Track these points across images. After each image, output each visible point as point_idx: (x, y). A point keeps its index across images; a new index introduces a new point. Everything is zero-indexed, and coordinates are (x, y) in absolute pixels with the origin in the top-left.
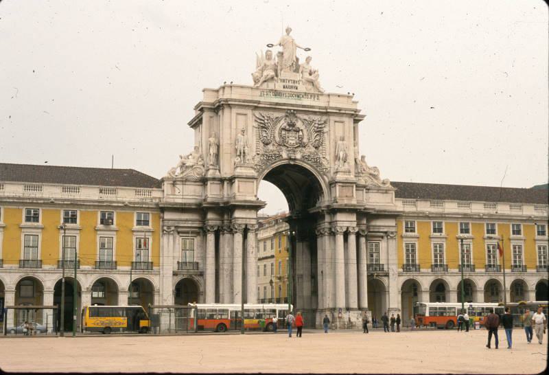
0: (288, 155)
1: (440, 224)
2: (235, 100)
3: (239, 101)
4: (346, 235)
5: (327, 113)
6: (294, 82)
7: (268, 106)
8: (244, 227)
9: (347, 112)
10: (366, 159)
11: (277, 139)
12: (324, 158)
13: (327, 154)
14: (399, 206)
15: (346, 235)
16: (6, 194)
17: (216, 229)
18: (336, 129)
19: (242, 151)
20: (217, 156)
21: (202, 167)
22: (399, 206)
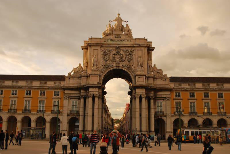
1: (193, 93)
2: (92, 44)
3: (94, 44)
4: (141, 98)
5: (134, 47)
6: (120, 35)
7: (107, 45)
8: (92, 95)
10: (156, 66)
11: (111, 58)
13: (134, 63)
14: (172, 85)
15: (141, 98)
16: (5, 85)
17: (84, 97)
18: (140, 53)
19: (94, 64)
20: (87, 67)
22: (172, 85)
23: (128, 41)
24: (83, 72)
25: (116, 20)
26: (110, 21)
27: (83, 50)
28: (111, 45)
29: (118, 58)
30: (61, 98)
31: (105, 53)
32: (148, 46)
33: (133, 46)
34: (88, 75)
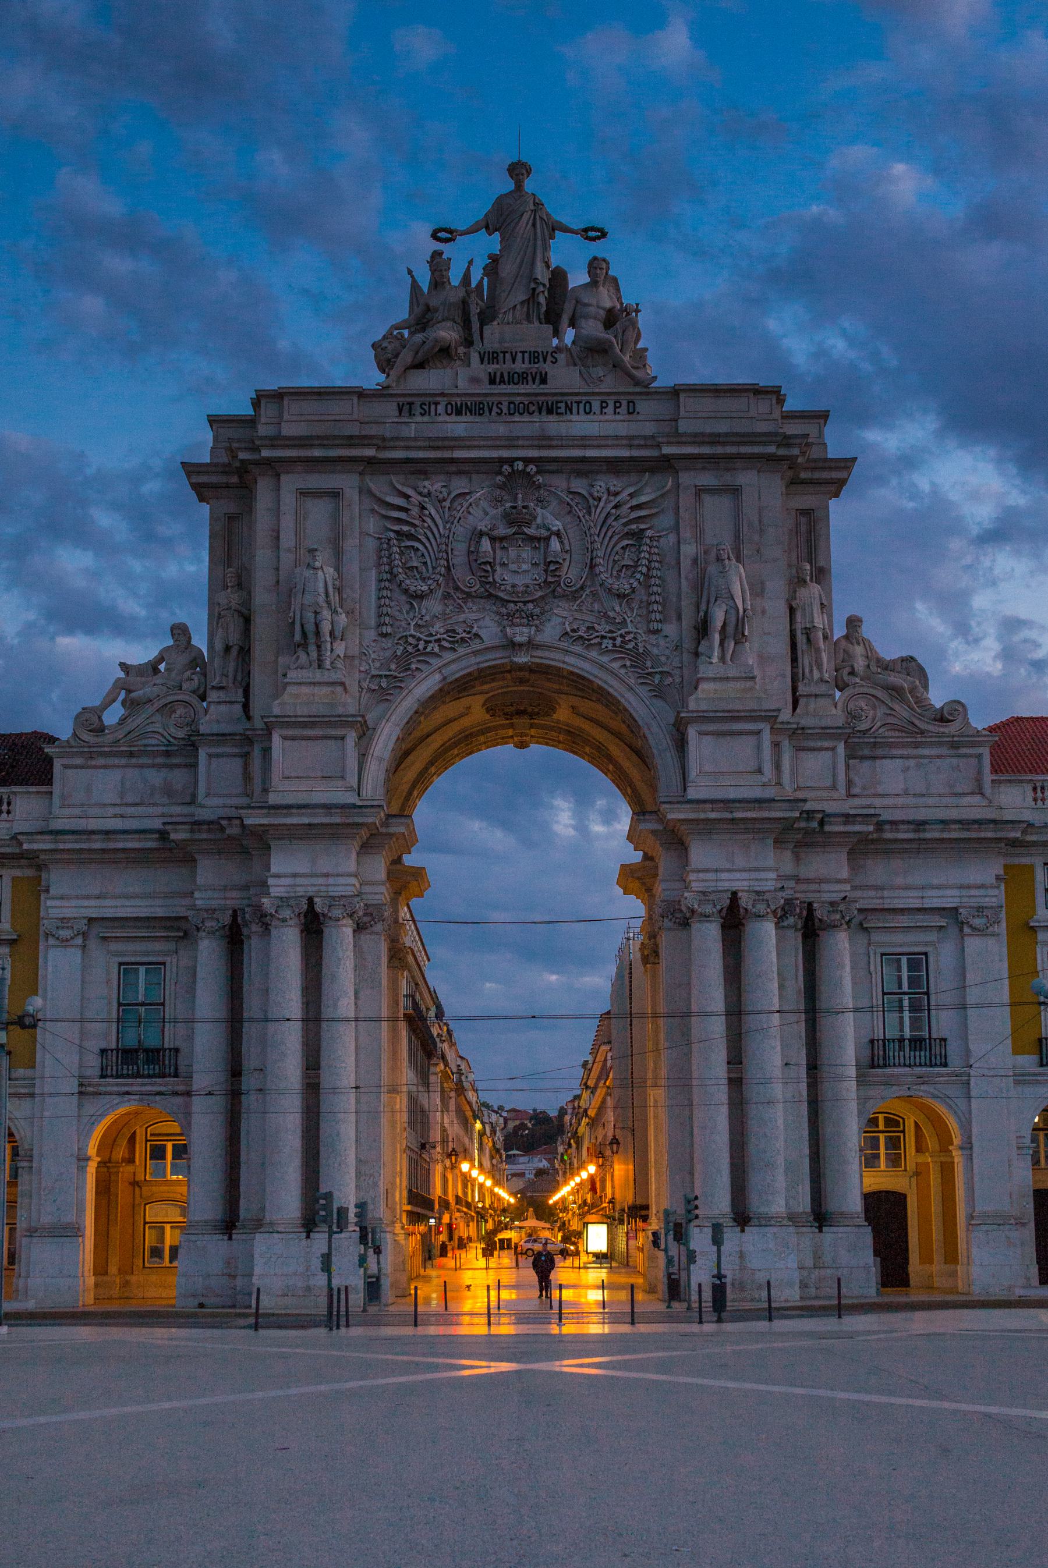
0: (503, 631)
6: (535, 357)
9: (744, 450)
10: (866, 631)
12: (657, 632)
19: (310, 628)
20: (245, 652)
21: (194, 700)
23: (610, 410)
24: (213, 696)
25: (489, 225)
26: (443, 234)
27: (202, 499)
28: (458, 454)
29: (525, 567)
30: (12, 943)
31: (406, 528)
32: (796, 451)
33: (654, 453)
34: (258, 723)
